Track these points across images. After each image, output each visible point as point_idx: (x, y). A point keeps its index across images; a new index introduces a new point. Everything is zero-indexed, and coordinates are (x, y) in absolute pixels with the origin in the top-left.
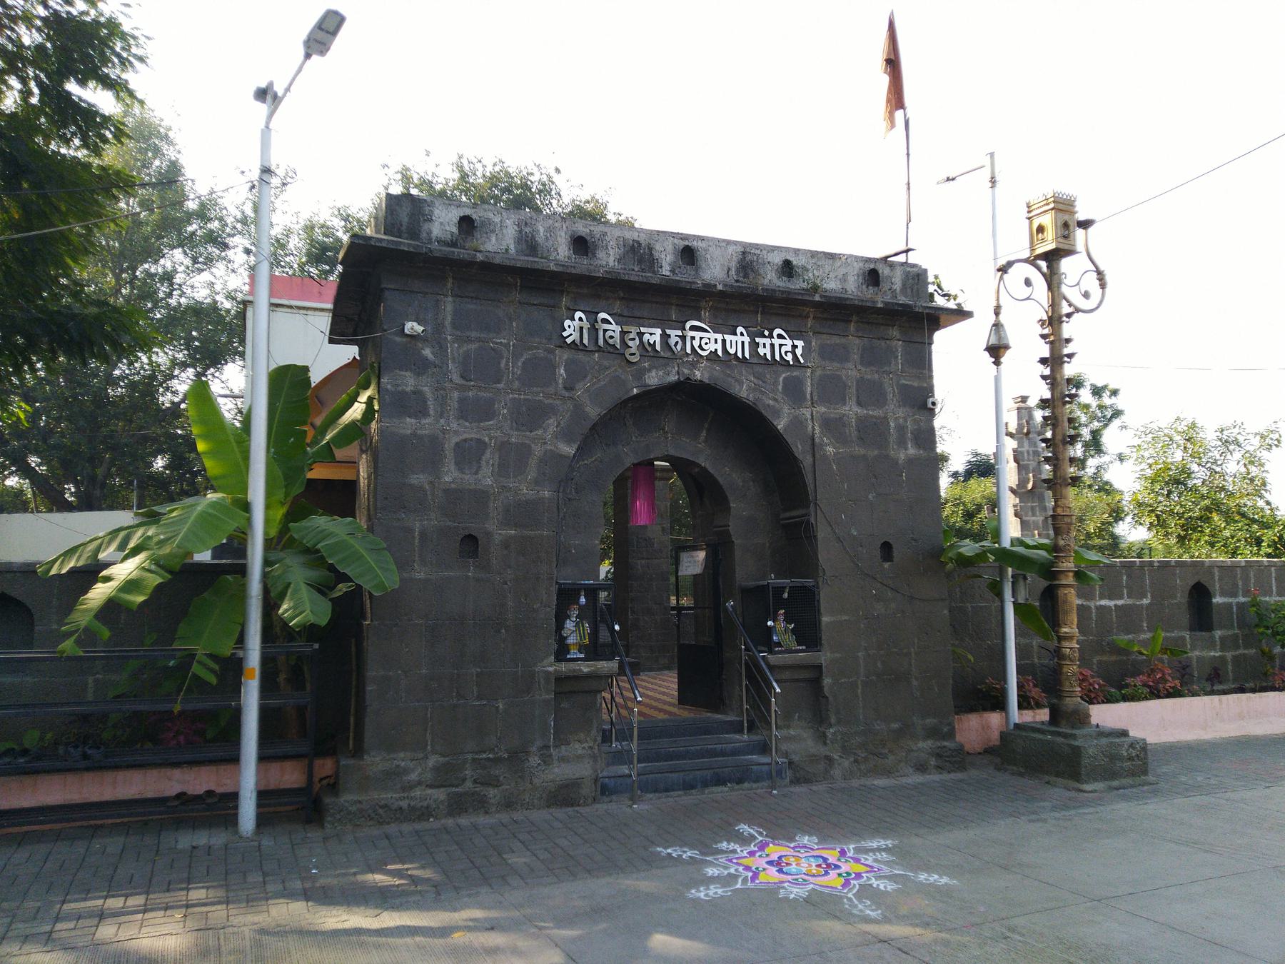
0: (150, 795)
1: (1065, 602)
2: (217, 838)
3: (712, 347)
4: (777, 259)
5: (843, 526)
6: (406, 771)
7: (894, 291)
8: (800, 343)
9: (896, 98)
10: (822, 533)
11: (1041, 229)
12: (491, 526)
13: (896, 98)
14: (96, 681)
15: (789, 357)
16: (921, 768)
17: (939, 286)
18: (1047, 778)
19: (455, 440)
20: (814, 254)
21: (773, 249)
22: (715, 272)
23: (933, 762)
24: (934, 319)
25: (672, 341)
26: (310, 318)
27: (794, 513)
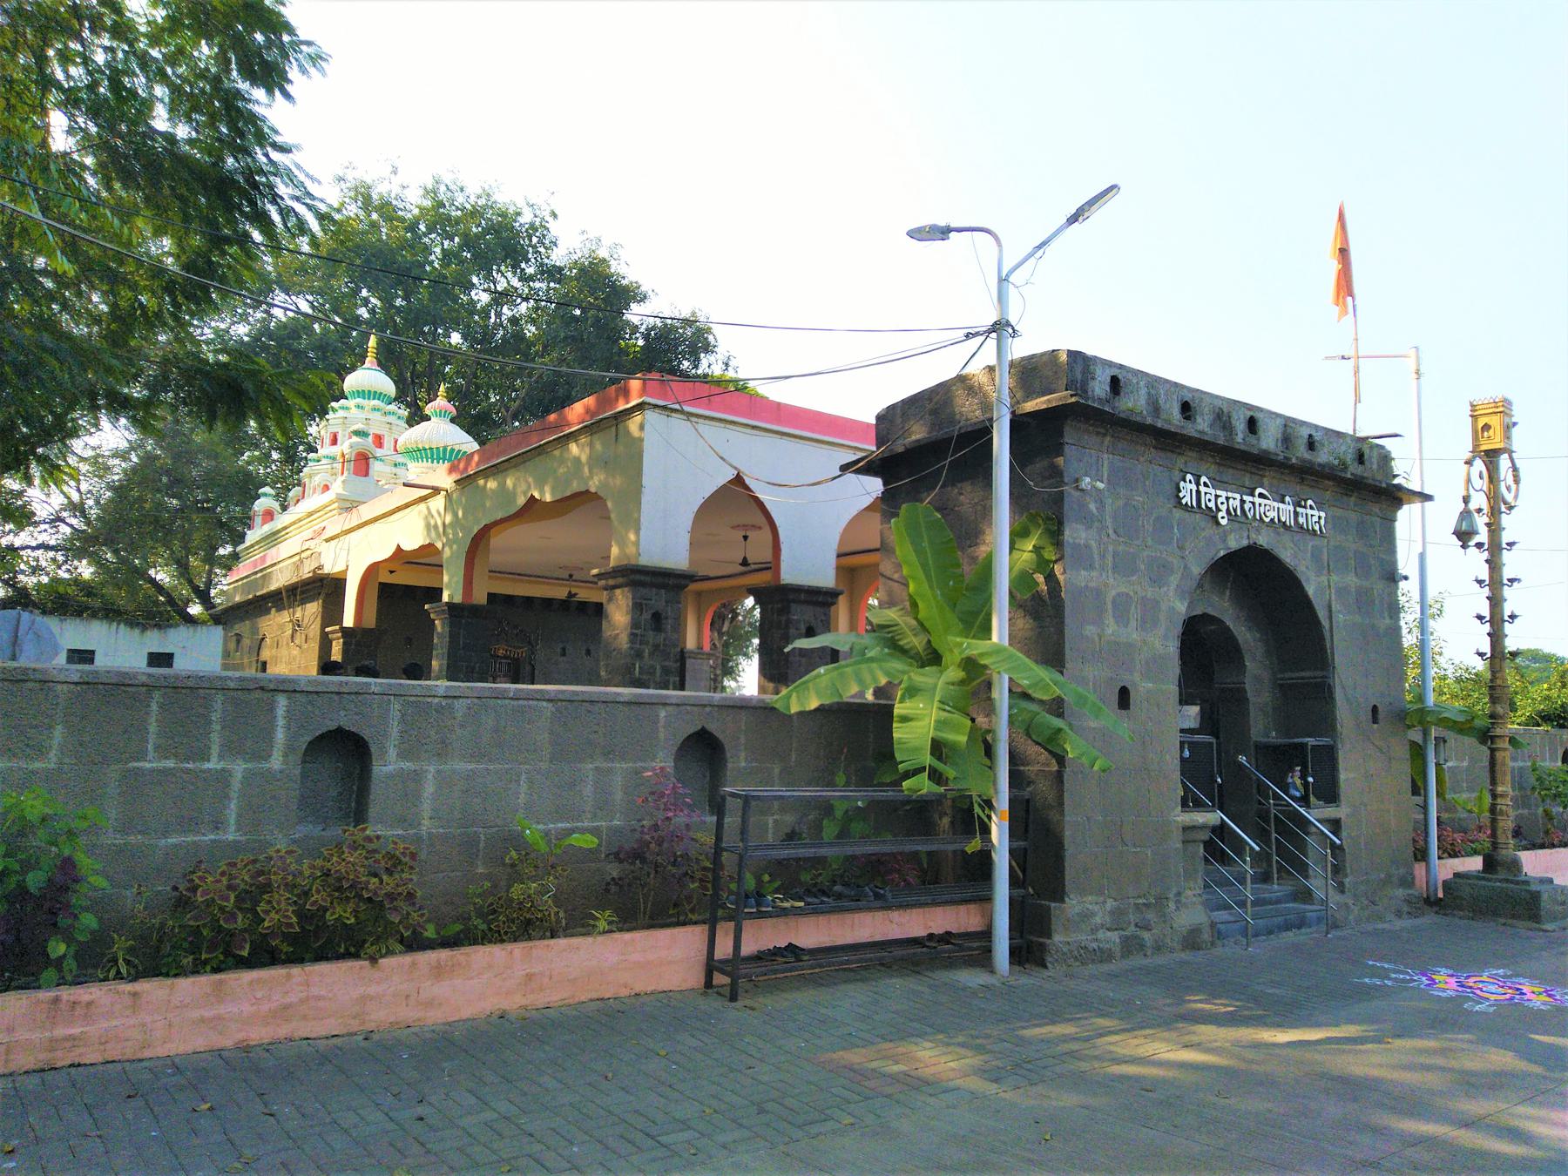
0: (878, 938)
1: (1504, 764)
2: (971, 978)
3: (1272, 514)
4: (1305, 432)
5: (1351, 683)
6: (1093, 914)
7: (1370, 471)
8: (1323, 514)
9: (1345, 284)
10: (1339, 695)
11: (1486, 427)
12: (1137, 677)
13: (1345, 284)
14: (775, 821)
15: (1317, 528)
16: (1399, 914)
17: (1469, 481)
18: (1502, 921)
19: (1114, 593)
20: (1328, 431)
21: (1303, 423)
22: (1268, 441)
23: (1405, 909)
24: (1392, 496)
25: (1247, 507)
26: (700, 427)
27: (1303, 674)
